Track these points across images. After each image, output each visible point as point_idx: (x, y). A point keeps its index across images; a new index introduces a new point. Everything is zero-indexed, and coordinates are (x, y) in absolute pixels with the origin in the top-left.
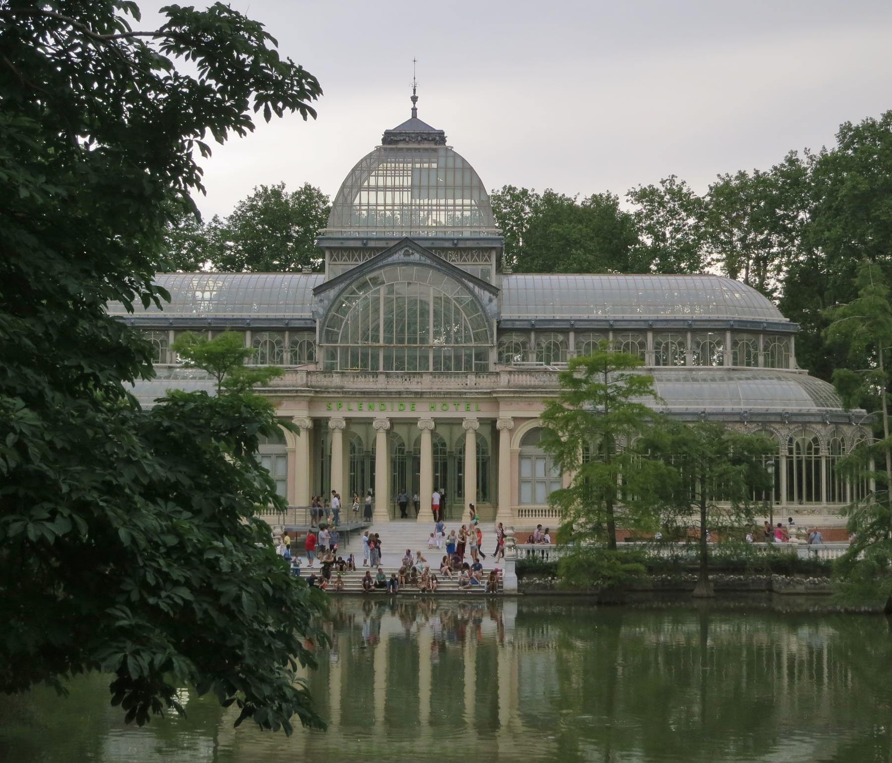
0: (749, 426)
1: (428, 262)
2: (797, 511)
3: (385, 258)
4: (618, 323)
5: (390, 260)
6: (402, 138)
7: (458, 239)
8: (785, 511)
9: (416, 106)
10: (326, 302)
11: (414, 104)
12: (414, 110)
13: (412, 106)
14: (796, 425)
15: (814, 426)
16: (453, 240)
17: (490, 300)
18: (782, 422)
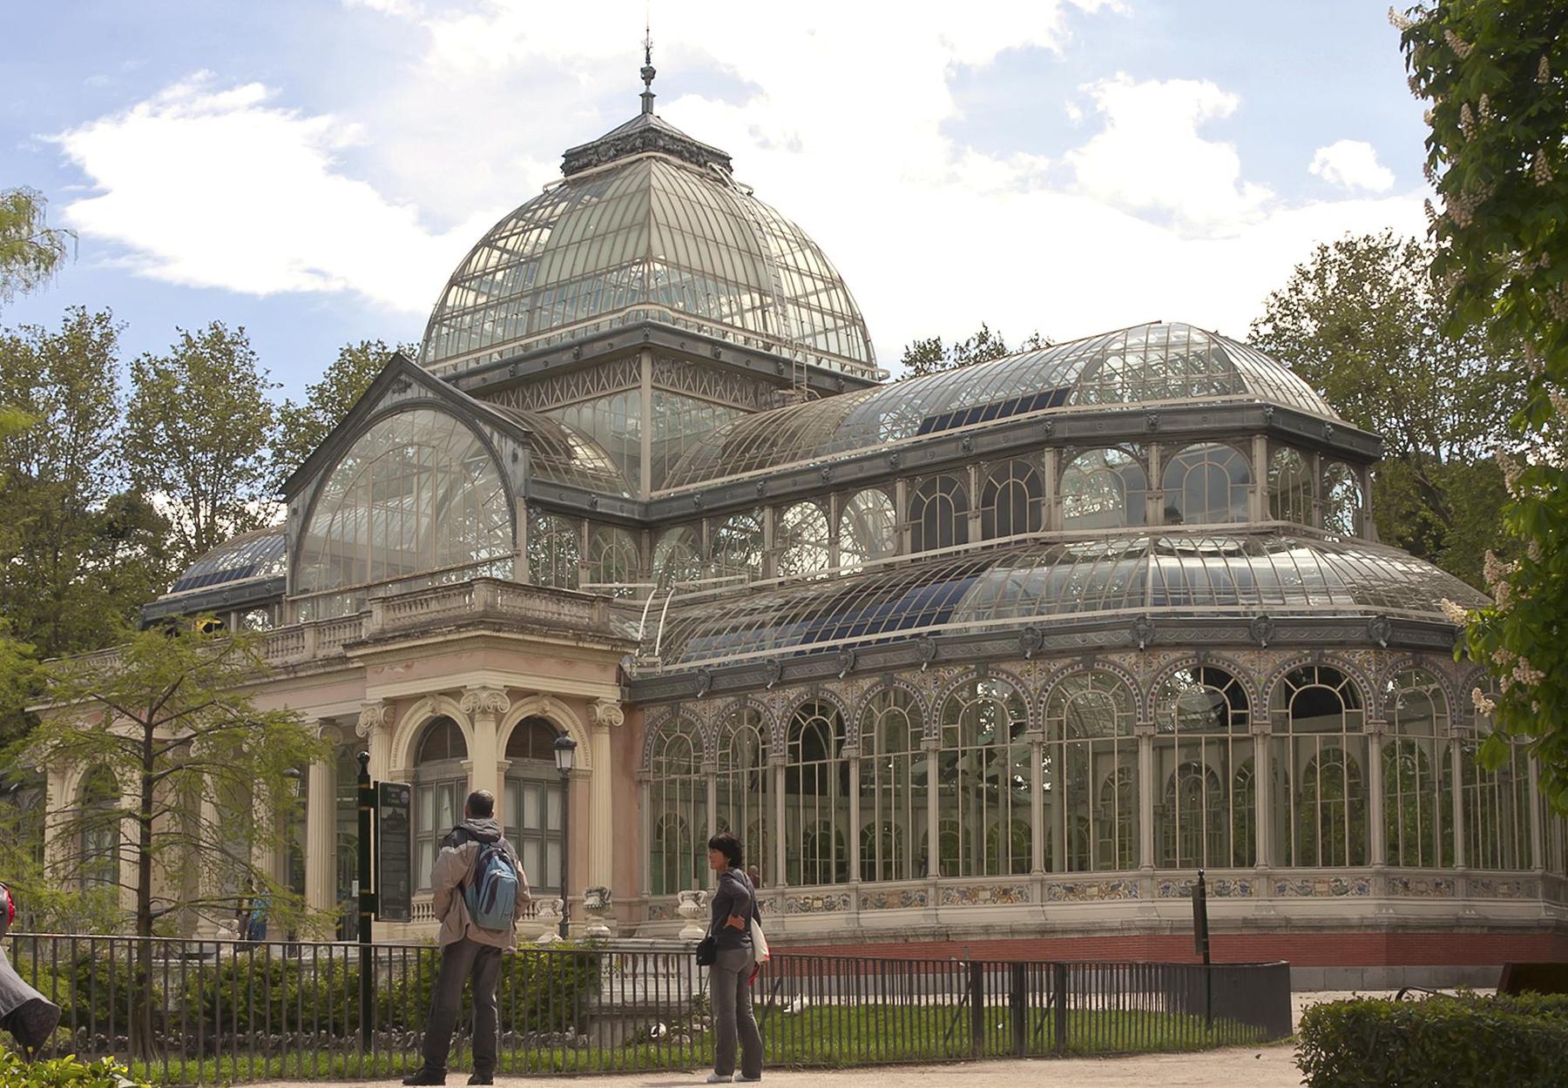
0: (944, 673)
1: (430, 395)
2: (1071, 890)
3: (371, 407)
4: (838, 472)
5: (381, 406)
6: (586, 161)
7: (581, 344)
8: (1037, 887)
9: (652, 90)
10: (300, 510)
11: (648, 84)
12: (648, 98)
13: (643, 89)
14: (1068, 661)
15: (1115, 658)
16: (569, 347)
17: (515, 457)
18: (1020, 657)
